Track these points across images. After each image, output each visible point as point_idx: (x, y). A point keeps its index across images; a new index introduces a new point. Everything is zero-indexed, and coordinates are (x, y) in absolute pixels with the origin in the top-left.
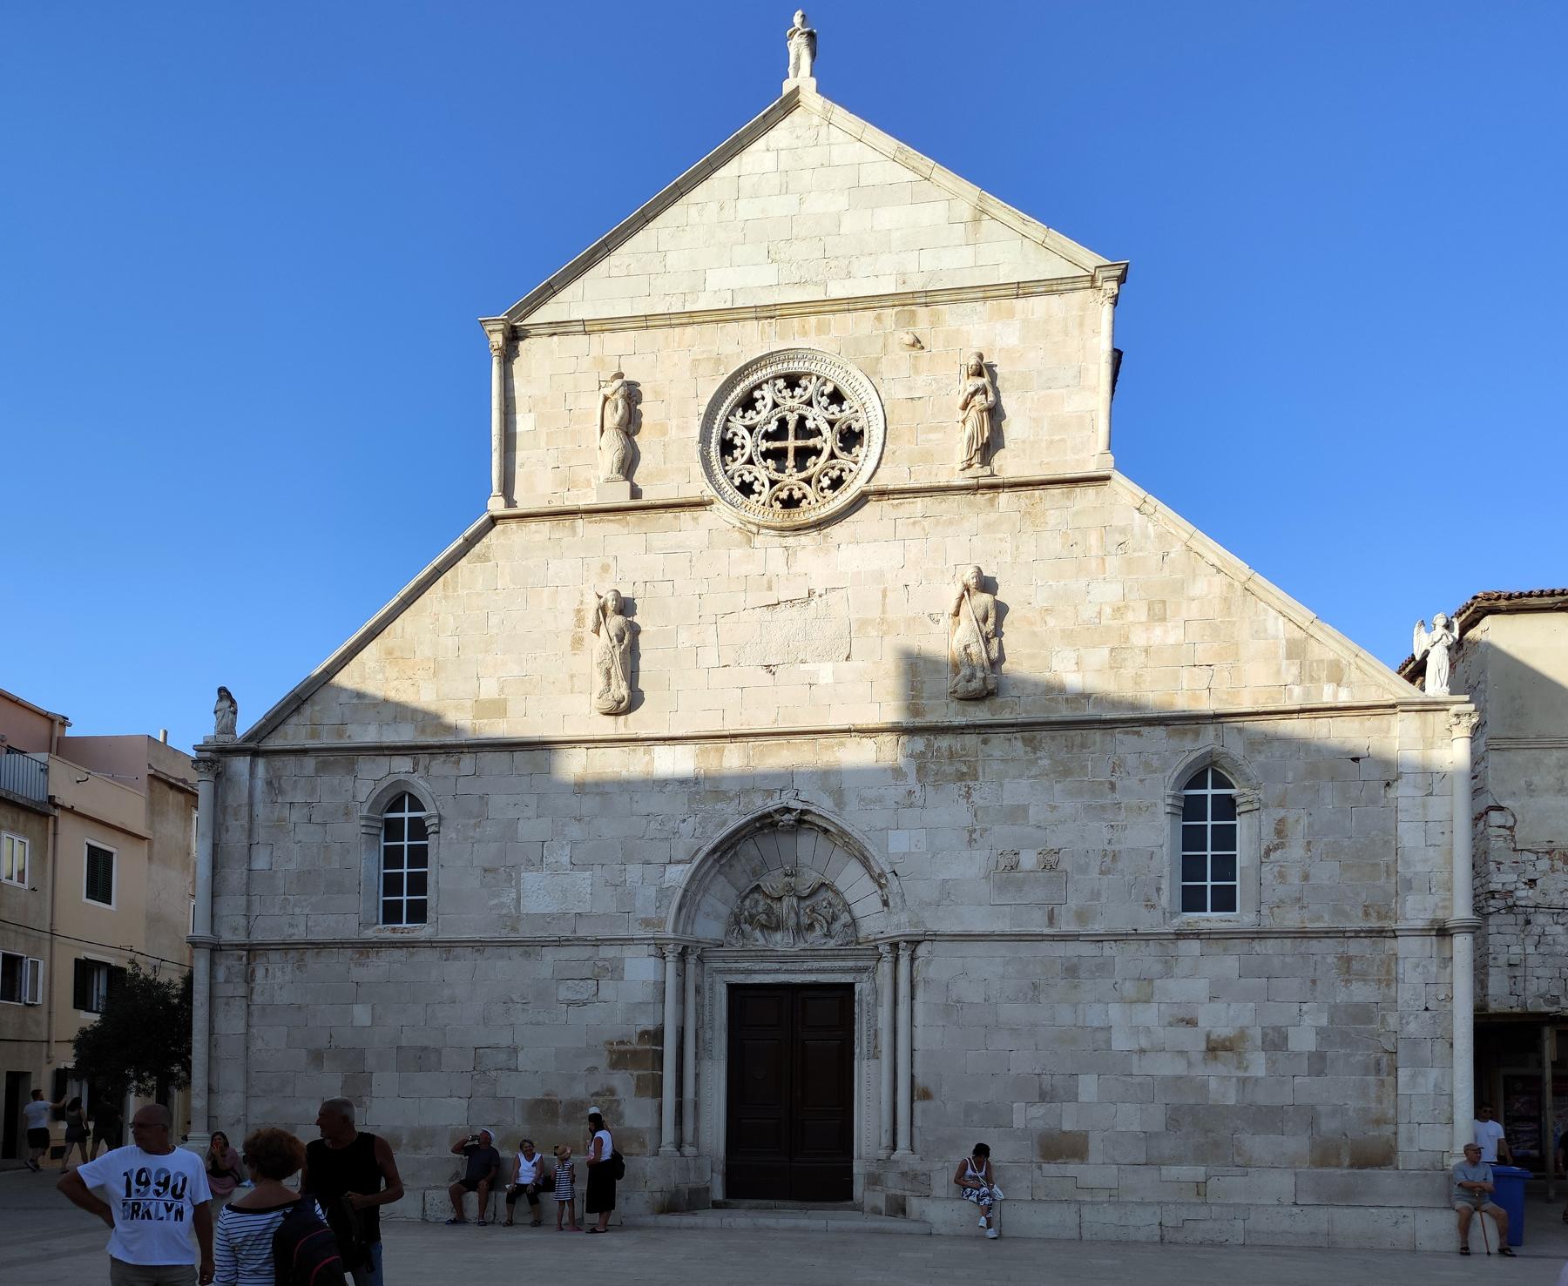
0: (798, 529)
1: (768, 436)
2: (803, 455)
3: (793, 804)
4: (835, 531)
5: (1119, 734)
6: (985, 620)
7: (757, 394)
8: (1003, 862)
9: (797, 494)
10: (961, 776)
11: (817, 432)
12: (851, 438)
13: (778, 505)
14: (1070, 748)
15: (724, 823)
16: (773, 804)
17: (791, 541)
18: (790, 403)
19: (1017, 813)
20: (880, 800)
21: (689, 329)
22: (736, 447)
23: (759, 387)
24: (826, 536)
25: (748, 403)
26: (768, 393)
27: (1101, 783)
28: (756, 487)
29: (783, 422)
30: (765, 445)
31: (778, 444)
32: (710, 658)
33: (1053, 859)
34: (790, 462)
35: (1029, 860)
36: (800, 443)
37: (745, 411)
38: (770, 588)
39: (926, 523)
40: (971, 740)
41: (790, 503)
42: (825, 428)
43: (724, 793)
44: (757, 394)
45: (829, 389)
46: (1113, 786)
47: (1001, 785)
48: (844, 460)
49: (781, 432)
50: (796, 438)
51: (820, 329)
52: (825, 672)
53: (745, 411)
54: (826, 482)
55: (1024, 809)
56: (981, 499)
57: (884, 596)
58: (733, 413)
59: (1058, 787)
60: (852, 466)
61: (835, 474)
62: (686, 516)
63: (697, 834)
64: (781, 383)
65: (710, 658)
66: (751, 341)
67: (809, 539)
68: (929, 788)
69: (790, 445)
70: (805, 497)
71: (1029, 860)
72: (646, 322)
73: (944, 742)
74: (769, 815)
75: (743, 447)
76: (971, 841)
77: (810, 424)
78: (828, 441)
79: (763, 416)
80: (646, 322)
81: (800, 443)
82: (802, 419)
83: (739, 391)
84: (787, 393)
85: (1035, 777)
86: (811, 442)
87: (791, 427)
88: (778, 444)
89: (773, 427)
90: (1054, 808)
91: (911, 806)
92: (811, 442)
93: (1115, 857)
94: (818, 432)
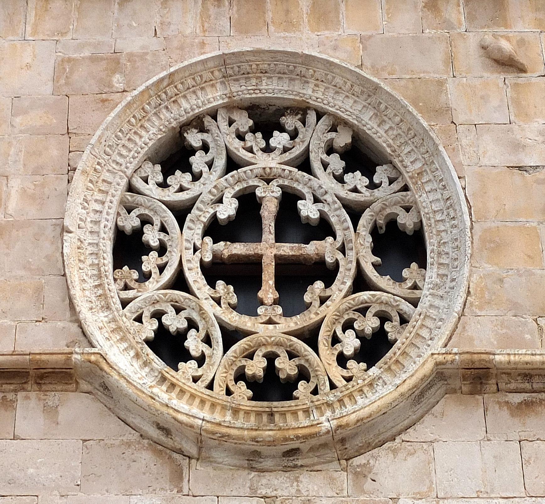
0: (292, 456)
1: (215, 230)
2: (296, 278)
7: (194, 138)
9: (286, 367)
11: (323, 229)
12: (400, 246)
13: (242, 390)
22: (147, 249)
26: (222, 136)
28: (193, 343)
29: (249, 202)
30: (210, 249)
31: (239, 249)
34: (268, 291)
36: (287, 249)
37: (167, 172)
41: (271, 387)
42: (339, 219)
45: (343, 139)
48: (388, 291)
50: (279, 238)
54: (350, 343)
61: (369, 324)
64: (244, 122)
69: (266, 255)
70: (303, 374)
75: (162, 250)
77: (308, 210)
78: (353, 248)
81: (287, 249)
84: (256, 141)
86: (312, 249)
87: (269, 211)
88: (239, 249)
92: (312, 249)
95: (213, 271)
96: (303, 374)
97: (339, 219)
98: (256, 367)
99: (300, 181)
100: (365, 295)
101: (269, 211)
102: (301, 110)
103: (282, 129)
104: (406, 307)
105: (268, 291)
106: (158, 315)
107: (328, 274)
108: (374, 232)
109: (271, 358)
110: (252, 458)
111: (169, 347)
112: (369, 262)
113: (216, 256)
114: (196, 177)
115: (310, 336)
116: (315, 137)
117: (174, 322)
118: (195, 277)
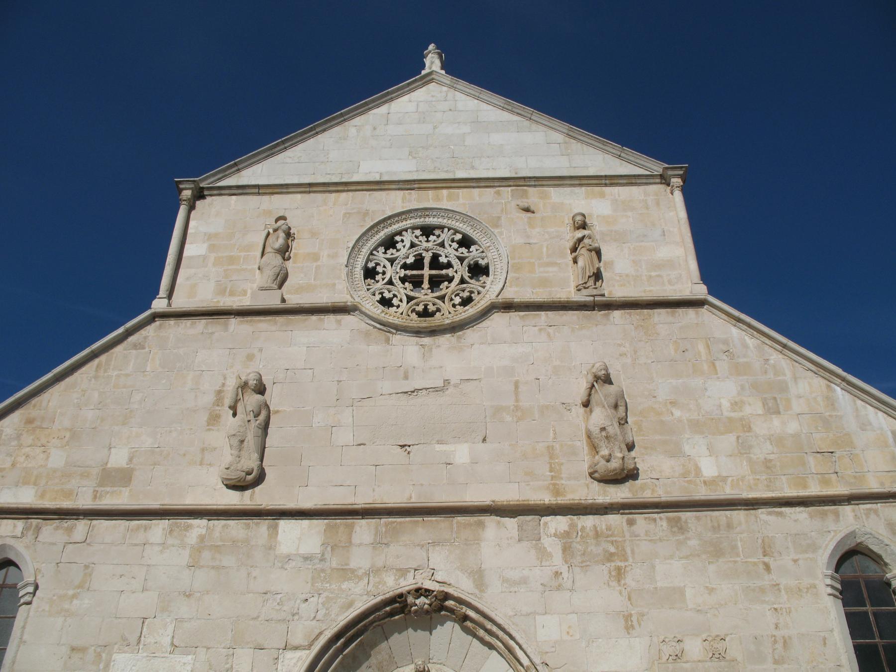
0: (433, 332)
3: (428, 585)
4: (470, 335)
5: (762, 513)
6: (616, 407)
7: (398, 238)
8: (667, 650)
9: (431, 308)
10: (610, 557)
11: (449, 265)
12: (478, 270)
14: (716, 529)
15: (350, 605)
16: (407, 584)
17: (427, 340)
18: (425, 245)
19: (673, 596)
20: (524, 581)
21: (344, 195)
22: (378, 273)
23: (400, 233)
24: (459, 338)
25: (390, 243)
26: (408, 238)
27: (755, 564)
28: (395, 301)
30: (403, 273)
32: (344, 436)
33: (720, 646)
35: (694, 648)
36: (434, 272)
37: (387, 249)
38: (406, 377)
39: (551, 330)
40: (614, 520)
42: (455, 262)
43: (353, 571)
44: (398, 238)
45: (458, 237)
46: (767, 567)
47: (653, 567)
48: (474, 284)
49: (418, 263)
51: (450, 198)
52: (461, 453)
53: (387, 249)
54: (457, 300)
55: (681, 592)
56: (598, 315)
57: (516, 385)
58: (376, 249)
59: (712, 568)
60: (480, 289)
61: (466, 294)
62: (331, 319)
63: (319, 616)
65: (344, 436)
66: (396, 202)
67: (445, 340)
68: (577, 570)
71: (694, 648)
72: (310, 188)
73: (588, 522)
74: (401, 596)
75: (384, 273)
76: (629, 628)
77: (443, 260)
78: (460, 271)
79: (404, 253)
80: (310, 188)
81: (434, 272)
82: (435, 257)
83: (382, 235)
85: (687, 557)
86: (444, 272)
87: (427, 262)
88: (415, 272)
89: (411, 260)
90: (711, 591)
91: (559, 588)
93: (786, 643)
94: (449, 265)
95: (403, 280)
96: (438, 310)
97: (455, 262)
98: (420, 308)
99: (440, 251)
100: (464, 285)
101: (427, 262)
102: (442, 228)
103: (434, 235)
104: (480, 289)
105: (426, 285)
106: (382, 293)
107: (450, 280)
108: (469, 266)
109: (426, 306)
110: (418, 332)
111: (386, 302)
112: (466, 275)
113: (405, 275)
114: (398, 251)
115: (442, 298)
116: (445, 236)
117: (387, 295)
118: (396, 281)
